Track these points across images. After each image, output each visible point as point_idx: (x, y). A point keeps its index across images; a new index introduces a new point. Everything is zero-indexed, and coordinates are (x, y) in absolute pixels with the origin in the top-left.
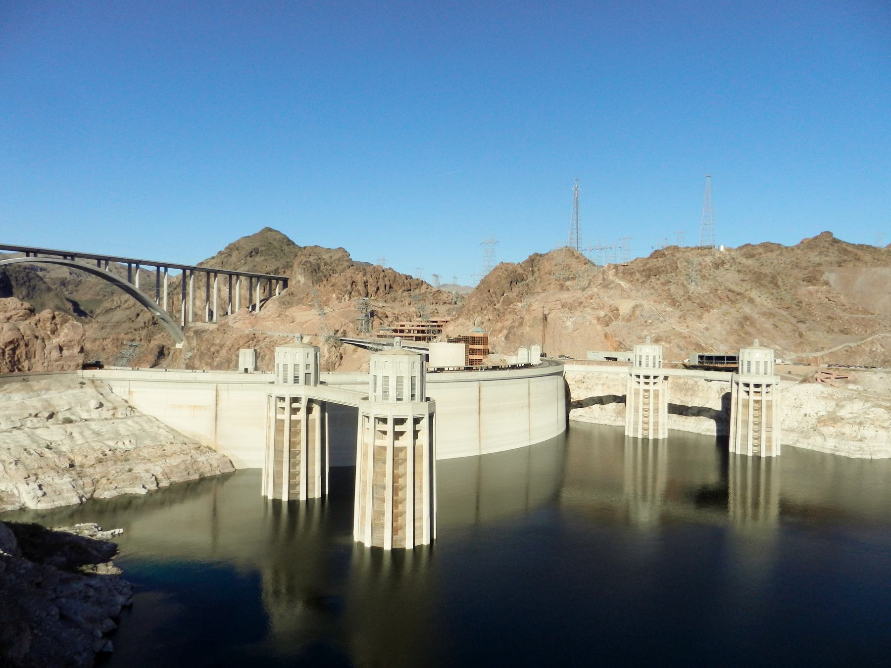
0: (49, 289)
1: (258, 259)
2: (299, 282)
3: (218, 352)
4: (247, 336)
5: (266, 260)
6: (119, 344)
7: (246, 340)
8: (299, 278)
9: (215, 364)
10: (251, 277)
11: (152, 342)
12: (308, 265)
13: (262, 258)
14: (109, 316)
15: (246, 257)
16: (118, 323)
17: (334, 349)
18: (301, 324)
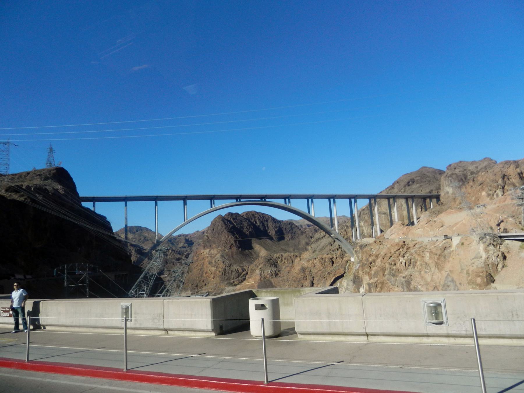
0: (303, 233)
1: (415, 186)
2: (448, 193)
3: (374, 261)
4: (398, 244)
5: (421, 186)
6: (323, 261)
7: (397, 248)
8: (448, 190)
9: (373, 273)
10: (407, 198)
11: (344, 259)
12: (454, 176)
13: (418, 185)
14: (319, 243)
15: (405, 186)
16: (323, 248)
17: (492, 247)
18: (451, 227)
